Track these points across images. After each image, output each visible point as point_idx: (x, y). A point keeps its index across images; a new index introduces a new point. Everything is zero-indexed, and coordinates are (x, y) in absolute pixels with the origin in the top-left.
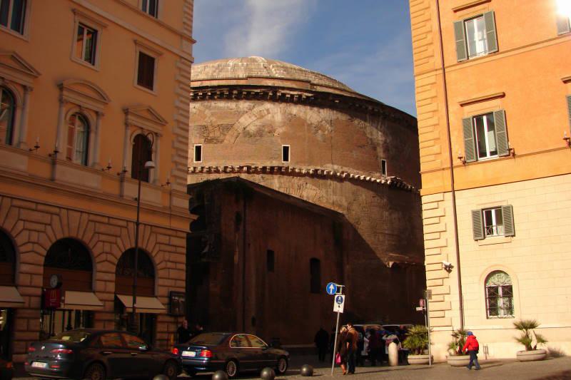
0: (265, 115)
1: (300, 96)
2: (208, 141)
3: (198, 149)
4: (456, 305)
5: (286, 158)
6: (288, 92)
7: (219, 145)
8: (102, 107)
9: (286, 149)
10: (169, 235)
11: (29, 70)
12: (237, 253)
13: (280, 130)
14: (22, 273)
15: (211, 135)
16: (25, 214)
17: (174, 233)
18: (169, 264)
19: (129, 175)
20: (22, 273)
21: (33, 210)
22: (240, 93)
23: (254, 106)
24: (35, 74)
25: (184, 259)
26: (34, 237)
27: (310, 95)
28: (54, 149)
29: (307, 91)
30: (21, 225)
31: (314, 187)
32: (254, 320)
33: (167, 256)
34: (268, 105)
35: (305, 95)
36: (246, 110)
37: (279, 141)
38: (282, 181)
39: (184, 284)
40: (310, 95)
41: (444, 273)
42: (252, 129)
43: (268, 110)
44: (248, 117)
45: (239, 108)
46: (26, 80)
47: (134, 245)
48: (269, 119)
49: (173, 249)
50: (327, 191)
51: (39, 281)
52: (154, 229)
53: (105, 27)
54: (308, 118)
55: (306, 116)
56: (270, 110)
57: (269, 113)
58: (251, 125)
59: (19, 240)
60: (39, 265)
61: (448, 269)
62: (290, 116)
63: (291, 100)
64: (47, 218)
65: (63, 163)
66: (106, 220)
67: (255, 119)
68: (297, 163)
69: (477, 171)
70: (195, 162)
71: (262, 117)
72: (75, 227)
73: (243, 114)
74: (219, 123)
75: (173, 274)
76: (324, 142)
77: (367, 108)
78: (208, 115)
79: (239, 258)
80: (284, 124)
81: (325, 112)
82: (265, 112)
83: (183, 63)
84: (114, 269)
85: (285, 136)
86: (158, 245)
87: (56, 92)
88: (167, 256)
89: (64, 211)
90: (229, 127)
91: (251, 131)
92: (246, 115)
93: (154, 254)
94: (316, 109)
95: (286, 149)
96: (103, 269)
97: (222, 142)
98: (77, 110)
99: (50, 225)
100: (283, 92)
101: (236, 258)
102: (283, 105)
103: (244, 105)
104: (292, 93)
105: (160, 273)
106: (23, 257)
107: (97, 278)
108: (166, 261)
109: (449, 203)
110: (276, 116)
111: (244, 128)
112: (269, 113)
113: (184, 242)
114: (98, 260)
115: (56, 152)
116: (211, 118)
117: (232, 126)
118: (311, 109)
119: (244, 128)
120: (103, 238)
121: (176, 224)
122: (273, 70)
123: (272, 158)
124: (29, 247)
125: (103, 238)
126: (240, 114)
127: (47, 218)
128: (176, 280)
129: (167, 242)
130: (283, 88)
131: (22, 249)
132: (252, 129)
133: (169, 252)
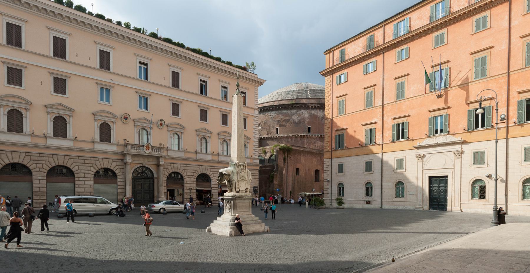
1: (315, 106)
2: (280, 126)
3: (277, 129)
5: (309, 131)
6: (310, 105)
7: (285, 128)
9: (309, 128)
11: (210, 132)
13: (307, 121)
15: (282, 124)
16: (212, 170)
17: (254, 170)
22: (292, 106)
23: (297, 112)
24: (211, 133)
25: (258, 177)
27: (319, 105)
29: (317, 104)
30: (211, 173)
32: (291, 192)
34: (303, 111)
36: (294, 113)
37: (307, 125)
38: (308, 140)
39: (258, 184)
40: (319, 105)
41: (327, 183)
42: (297, 120)
43: (303, 113)
46: (209, 135)
48: (303, 116)
49: (254, 175)
57: (303, 114)
58: (296, 119)
59: (211, 177)
61: (328, 181)
63: (312, 108)
65: (221, 155)
67: (298, 116)
68: (314, 133)
69: (339, 153)
70: (276, 134)
71: (300, 116)
73: (293, 115)
74: (284, 119)
80: (309, 118)
82: (302, 114)
83: (256, 118)
85: (309, 123)
90: (287, 121)
91: (296, 122)
92: (294, 116)
94: (322, 111)
95: (309, 128)
97: (286, 126)
98: (224, 140)
100: (308, 105)
101: (284, 172)
102: (308, 110)
103: (293, 111)
104: (312, 105)
106: (212, 181)
109: (330, 162)
110: (306, 115)
111: (294, 121)
113: (258, 173)
115: (219, 153)
117: (289, 120)
118: (320, 111)
121: (255, 168)
124: (214, 178)
126: (292, 115)
132: (297, 120)
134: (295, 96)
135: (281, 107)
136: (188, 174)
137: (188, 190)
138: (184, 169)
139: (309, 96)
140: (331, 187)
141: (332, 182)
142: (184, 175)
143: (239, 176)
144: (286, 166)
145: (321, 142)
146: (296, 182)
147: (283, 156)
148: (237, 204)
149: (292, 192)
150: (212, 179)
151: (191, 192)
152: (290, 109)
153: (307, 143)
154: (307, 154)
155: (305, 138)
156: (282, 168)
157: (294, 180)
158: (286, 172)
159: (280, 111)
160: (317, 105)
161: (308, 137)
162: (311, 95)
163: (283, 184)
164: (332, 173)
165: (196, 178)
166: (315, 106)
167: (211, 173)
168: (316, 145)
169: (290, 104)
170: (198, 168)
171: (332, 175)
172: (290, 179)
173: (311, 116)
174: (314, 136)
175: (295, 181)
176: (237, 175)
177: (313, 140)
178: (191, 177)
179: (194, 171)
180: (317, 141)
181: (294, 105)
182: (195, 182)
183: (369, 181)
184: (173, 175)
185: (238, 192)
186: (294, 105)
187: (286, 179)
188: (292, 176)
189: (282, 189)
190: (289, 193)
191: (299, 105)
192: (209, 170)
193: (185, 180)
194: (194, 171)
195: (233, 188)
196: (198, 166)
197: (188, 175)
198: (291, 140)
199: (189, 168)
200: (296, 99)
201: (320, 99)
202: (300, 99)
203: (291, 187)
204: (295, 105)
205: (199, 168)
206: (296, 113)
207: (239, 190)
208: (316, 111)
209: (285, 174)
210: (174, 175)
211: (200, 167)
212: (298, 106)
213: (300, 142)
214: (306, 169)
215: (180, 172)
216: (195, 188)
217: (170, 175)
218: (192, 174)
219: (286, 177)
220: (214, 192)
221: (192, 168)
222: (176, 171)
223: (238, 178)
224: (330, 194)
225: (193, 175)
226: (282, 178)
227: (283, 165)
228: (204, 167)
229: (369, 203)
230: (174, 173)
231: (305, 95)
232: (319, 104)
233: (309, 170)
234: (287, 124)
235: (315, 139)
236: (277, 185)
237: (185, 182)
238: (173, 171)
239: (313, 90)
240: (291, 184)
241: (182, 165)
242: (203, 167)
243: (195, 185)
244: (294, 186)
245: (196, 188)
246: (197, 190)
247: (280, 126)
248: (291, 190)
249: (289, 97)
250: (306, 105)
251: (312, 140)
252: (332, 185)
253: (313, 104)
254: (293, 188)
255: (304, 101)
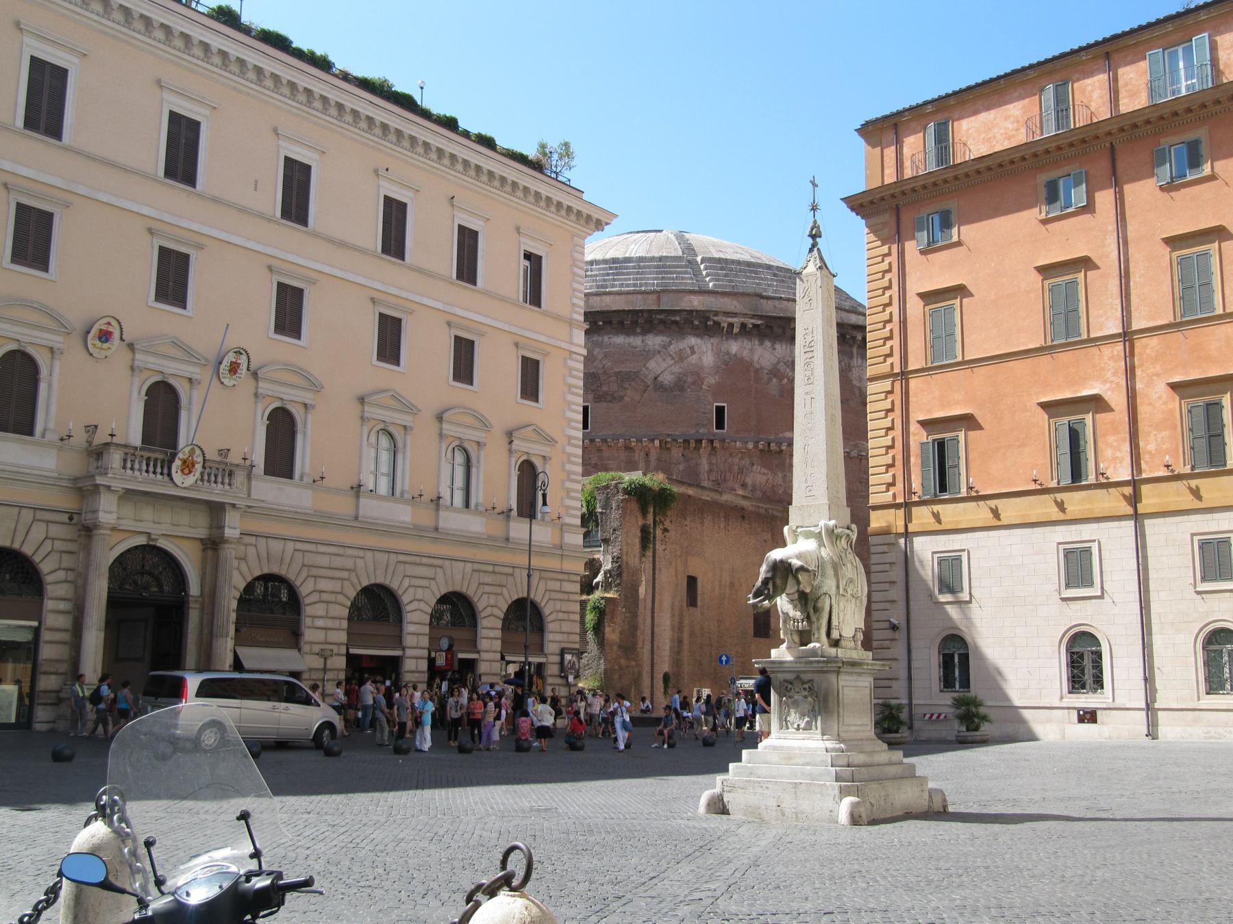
0: (688, 357)
1: (743, 326)
4: (903, 674)
5: (720, 425)
6: (724, 318)
8: (483, 435)
9: (720, 411)
10: (560, 580)
12: (644, 582)
13: (712, 380)
14: (409, 634)
15: (605, 388)
16: (411, 570)
18: (561, 616)
19: (514, 513)
20: (409, 634)
21: (418, 564)
23: (670, 343)
26: (419, 596)
27: (759, 322)
28: (437, 495)
29: (753, 316)
30: (406, 582)
31: (764, 470)
32: (666, 678)
33: (558, 606)
34: (693, 340)
35: (750, 322)
36: (657, 347)
37: (710, 398)
41: (889, 634)
42: (667, 379)
43: (692, 348)
44: (660, 360)
45: (647, 344)
46: (405, 419)
47: (525, 595)
48: (694, 362)
49: (565, 596)
50: (785, 476)
51: (425, 642)
52: (544, 574)
53: (482, 335)
54: (756, 358)
55: (753, 354)
56: (696, 348)
57: (693, 352)
60: (425, 624)
61: (894, 628)
62: (727, 357)
63: (729, 333)
64: (429, 572)
66: (490, 568)
67: (671, 362)
72: (457, 579)
73: (654, 355)
74: (616, 370)
75: (566, 627)
76: (782, 396)
77: (854, 338)
78: (600, 357)
79: (646, 591)
81: (784, 347)
84: (499, 624)
85: (718, 391)
86: (547, 593)
87: (435, 425)
88: (558, 606)
89: (447, 563)
91: (666, 382)
92: (658, 358)
93: (543, 604)
94: (768, 344)
95: (720, 411)
96: (489, 626)
97: (621, 398)
99: (433, 579)
100: (716, 318)
102: (714, 340)
103: (654, 341)
104: (730, 320)
105: (550, 627)
107: (483, 636)
108: (557, 612)
110: (704, 358)
111: (656, 378)
112: (693, 352)
114: (483, 615)
115: (439, 498)
116: (604, 363)
117: (637, 374)
118: (761, 344)
119: (656, 378)
120: (488, 589)
122: (702, 267)
123: (697, 425)
125: (488, 589)
126: (647, 355)
127: (429, 572)
128: (569, 633)
129: (559, 589)
130: (716, 313)
131: (409, 608)
133: (561, 600)
134: (652, 282)
135: (603, 322)
136: (323, 585)
137: (317, 656)
138: (306, 562)
139: (711, 284)
140: (909, 651)
141: (913, 631)
142: (304, 590)
143: (842, 580)
144: (649, 566)
145: (766, 471)
146: (686, 635)
147: (640, 523)
148: (841, 691)
149: (672, 677)
150: (409, 608)
151: (328, 666)
152: (639, 330)
153: (711, 471)
154: (725, 518)
155: (701, 450)
156: (636, 573)
157: (678, 628)
158: (650, 591)
159: (595, 339)
160: (753, 321)
161: (714, 448)
162: (717, 280)
163: (639, 646)
164: (911, 592)
165: (349, 604)
166: (743, 326)
167: (406, 582)
168: (749, 481)
169: (641, 311)
170: (358, 560)
171: (911, 603)
172: (665, 622)
173: (726, 363)
174: (738, 444)
175: (681, 630)
176: (836, 575)
177: (736, 460)
178: (331, 598)
179: (345, 574)
180: (753, 464)
181: (658, 317)
182: (345, 624)
183: (1083, 628)
184: (259, 590)
185: (836, 643)
186: (658, 317)
187: (649, 621)
188: (673, 609)
189: (633, 663)
190: (660, 684)
191: (678, 318)
192: (401, 567)
193: (308, 610)
194: (345, 574)
195: (819, 629)
196: (361, 553)
197: (321, 592)
198: (643, 454)
199: (324, 560)
200: (663, 291)
201: (758, 298)
202: (680, 295)
203: (667, 659)
204: (662, 317)
205: (363, 560)
206: (665, 347)
207: (840, 636)
208: (747, 344)
209: (645, 600)
210: (266, 589)
211: (369, 554)
212: (676, 323)
213: (681, 467)
214: (720, 581)
215: (291, 576)
216: (343, 650)
217: (249, 588)
218: (337, 586)
219: (649, 614)
220: (413, 668)
221: (338, 562)
222: (275, 569)
223: (838, 587)
224: (904, 683)
225: (338, 589)
226: (635, 615)
227: (637, 560)
228: (382, 557)
229: (1088, 716)
230: (266, 578)
231: (691, 279)
232: (761, 317)
233: (732, 585)
234: (629, 392)
235: (742, 458)
236: (615, 648)
237: (308, 621)
238: (266, 571)
239: (719, 260)
240: (667, 647)
241: (299, 546)
242: (378, 555)
243: (343, 637)
244: (679, 653)
245: (348, 651)
246: (351, 659)
247: (595, 398)
248: (666, 670)
249: (628, 282)
250: (708, 319)
251: (730, 460)
252: (914, 644)
253: (735, 315)
254: (677, 662)
255: (696, 303)
